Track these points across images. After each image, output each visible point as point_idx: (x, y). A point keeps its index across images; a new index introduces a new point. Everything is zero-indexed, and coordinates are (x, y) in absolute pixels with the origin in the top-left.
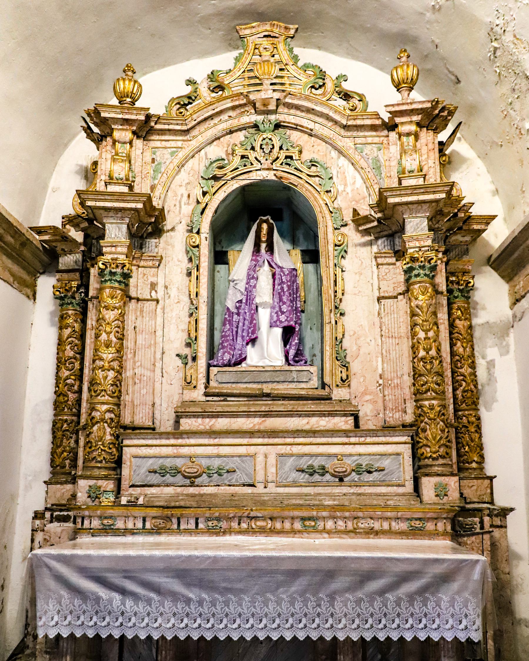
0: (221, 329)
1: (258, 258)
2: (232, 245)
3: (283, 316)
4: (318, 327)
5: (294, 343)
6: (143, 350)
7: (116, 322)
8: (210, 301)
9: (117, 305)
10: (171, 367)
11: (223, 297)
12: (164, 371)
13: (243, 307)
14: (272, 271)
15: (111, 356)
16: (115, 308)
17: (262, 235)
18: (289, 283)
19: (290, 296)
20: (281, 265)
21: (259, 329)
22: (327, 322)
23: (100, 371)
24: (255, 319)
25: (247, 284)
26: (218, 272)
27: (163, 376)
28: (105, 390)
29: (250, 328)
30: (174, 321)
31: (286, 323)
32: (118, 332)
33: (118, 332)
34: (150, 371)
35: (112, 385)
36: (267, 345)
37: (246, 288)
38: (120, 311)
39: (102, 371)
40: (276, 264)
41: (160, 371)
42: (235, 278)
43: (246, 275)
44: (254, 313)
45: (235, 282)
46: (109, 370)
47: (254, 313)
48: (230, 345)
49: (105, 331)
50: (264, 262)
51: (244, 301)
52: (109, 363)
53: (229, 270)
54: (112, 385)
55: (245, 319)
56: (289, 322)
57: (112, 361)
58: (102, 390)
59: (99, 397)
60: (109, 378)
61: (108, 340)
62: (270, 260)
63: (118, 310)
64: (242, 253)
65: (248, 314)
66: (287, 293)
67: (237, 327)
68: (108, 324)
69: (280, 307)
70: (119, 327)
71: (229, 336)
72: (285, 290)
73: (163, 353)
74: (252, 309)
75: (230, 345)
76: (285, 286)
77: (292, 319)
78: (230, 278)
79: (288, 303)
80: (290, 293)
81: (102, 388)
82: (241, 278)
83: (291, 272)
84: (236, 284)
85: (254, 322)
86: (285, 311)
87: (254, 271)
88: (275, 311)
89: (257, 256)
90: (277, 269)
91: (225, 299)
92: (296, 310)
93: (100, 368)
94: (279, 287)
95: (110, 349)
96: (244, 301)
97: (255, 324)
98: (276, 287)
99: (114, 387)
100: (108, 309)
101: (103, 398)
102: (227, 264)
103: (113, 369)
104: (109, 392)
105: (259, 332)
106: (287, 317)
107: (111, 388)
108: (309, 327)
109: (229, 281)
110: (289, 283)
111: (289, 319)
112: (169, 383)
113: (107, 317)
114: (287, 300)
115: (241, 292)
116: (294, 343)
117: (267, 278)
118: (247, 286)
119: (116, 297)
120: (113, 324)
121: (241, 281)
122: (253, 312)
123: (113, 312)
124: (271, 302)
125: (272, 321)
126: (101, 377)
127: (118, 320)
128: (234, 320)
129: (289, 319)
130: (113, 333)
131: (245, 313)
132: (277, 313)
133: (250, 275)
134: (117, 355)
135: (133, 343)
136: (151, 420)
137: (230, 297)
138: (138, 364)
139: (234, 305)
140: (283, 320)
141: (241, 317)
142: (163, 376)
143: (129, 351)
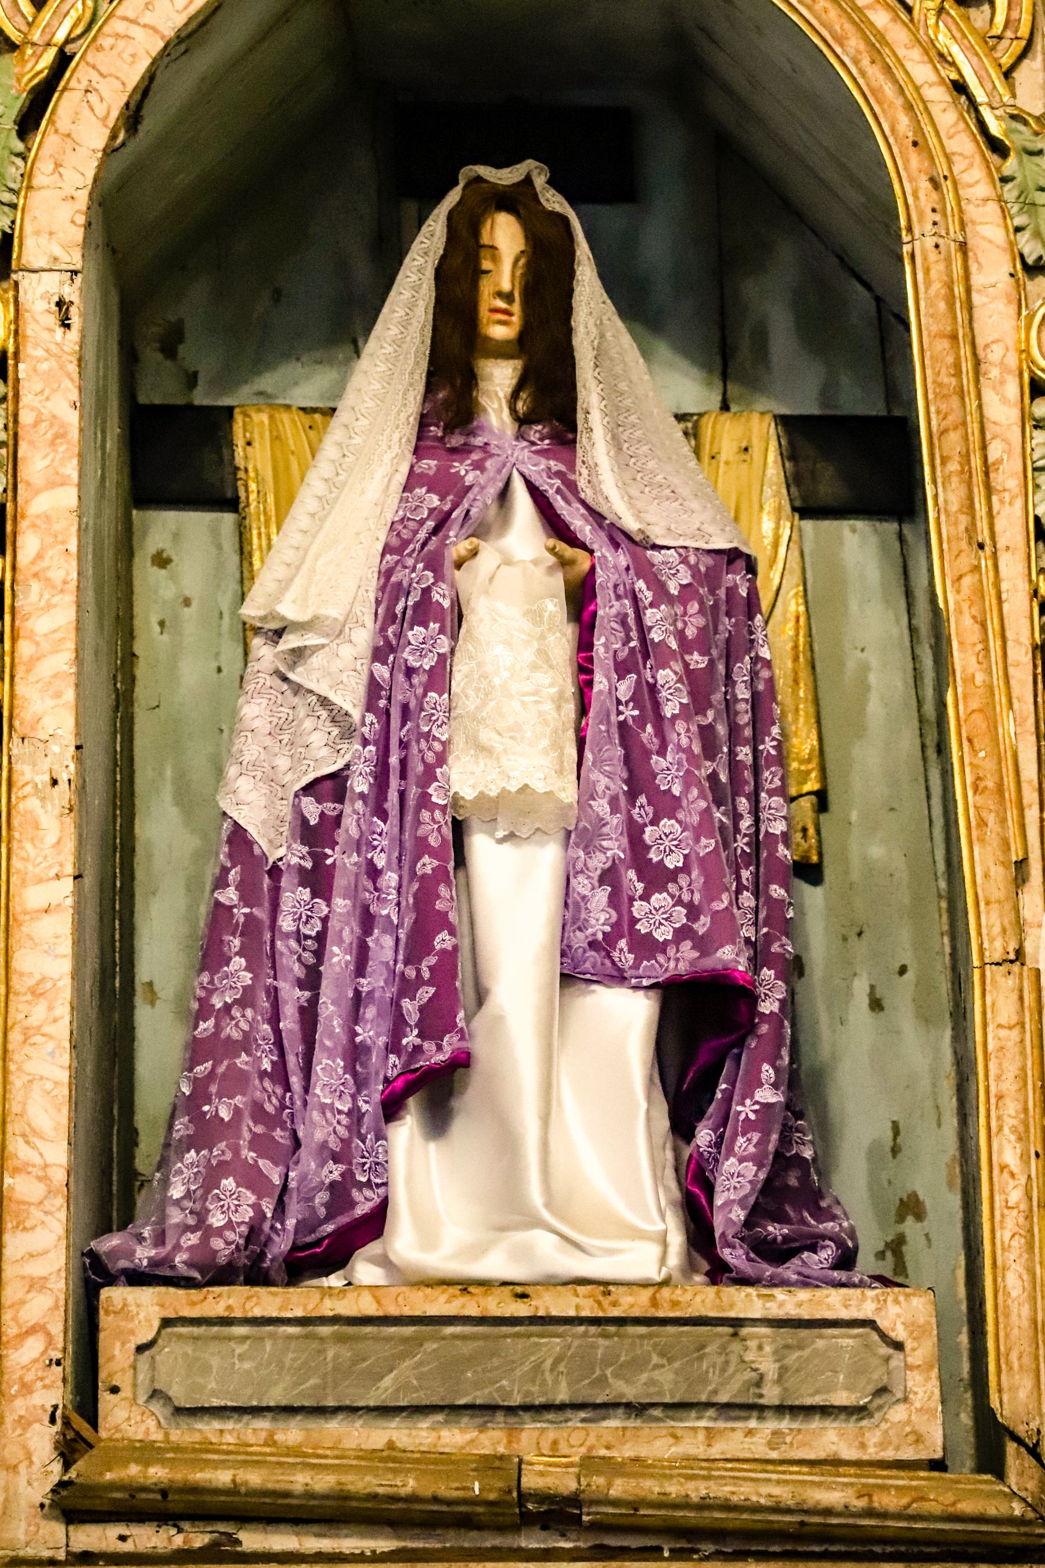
0: (180, 999)
1: (460, 468)
2: (260, 364)
3: (659, 899)
4: (923, 985)
5: (746, 1110)
8: (98, 782)
11: (198, 759)
13: (350, 826)
14: (564, 563)
17: (488, 301)
18: (697, 660)
19: (710, 750)
20: (631, 524)
21: (481, 997)
22: (996, 950)
24: (444, 923)
25: (379, 655)
26: (161, 561)
29: (407, 988)
31: (687, 950)
36: (546, 1119)
37: (374, 687)
40: (596, 516)
42: (289, 610)
43: (372, 584)
44: (440, 875)
45: (290, 641)
47: (440, 875)
48: (258, 1112)
50: (504, 495)
51: (360, 784)
53: (244, 552)
55: (367, 920)
56: (704, 945)
62: (550, 487)
64: (336, 432)
65: (390, 879)
66: (683, 734)
67: (312, 980)
69: (634, 833)
71: (246, 1044)
72: (670, 710)
74: (422, 846)
75: (258, 1112)
76: (666, 676)
77: (726, 924)
78: (251, 610)
79: (696, 803)
80: (706, 733)
82: (334, 612)
83: (711, 579)
84: (298, 655)
85: (442, 941)
86: (673, 862)
87: (434, 564)
88: (598, 862)
89: (462, 451)
90: (603, 550)
91: (219, 773)
92: (754, 857)
94: (625, 688)
96: (360, 784)
97: (450, 957)
98: (601, 682)
102: (232, 504)
105: (477, 1023)
106: (693, 912)
108: (861, 988)
109: (247, 631)
110: (697, 660)
111: (702, 925)
114: (688, 780)
115: (338, 717)
116: (746, 1110)
117: (535, 616)
118: (382, 672)
121: (339, 632)
122: (427, 865)
124: (569, 794)
125: (579, 940)
128: (286, 924)
129: (702, 925)
131: (374, 873)
132: (609, 877)
133: (400, 591)
137: (250, 749)
139: (285, 810)
140: (664, 934)
141: (341, 904)
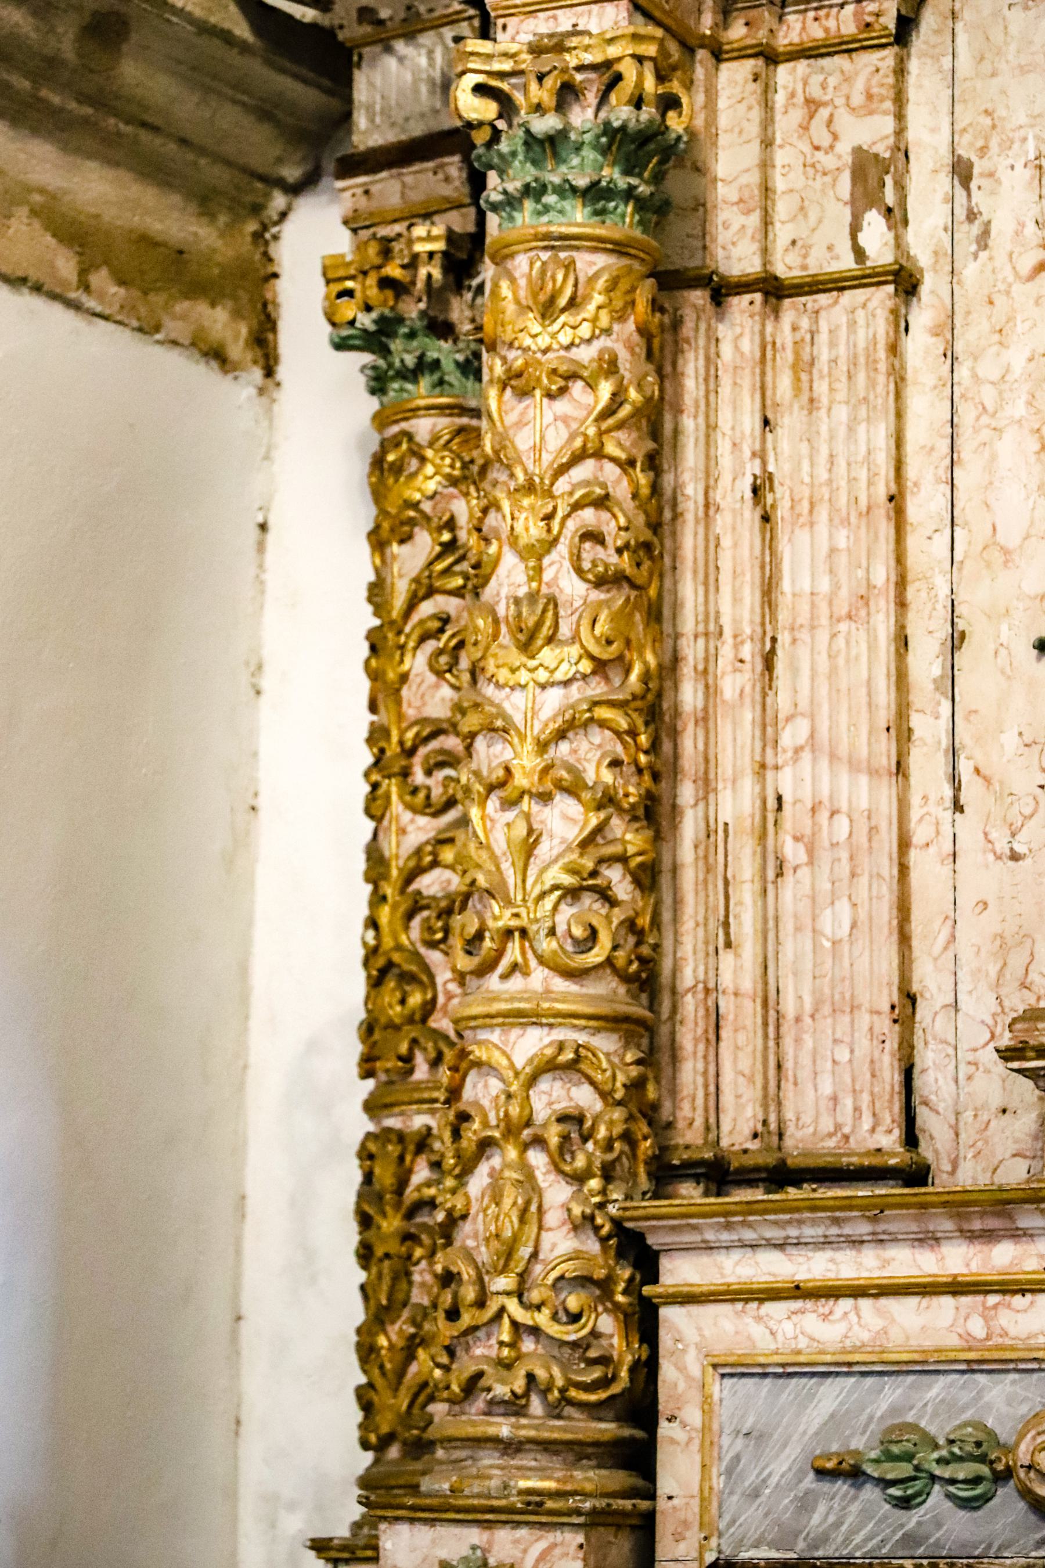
6: (823, 636)
7: (584, 470)
9: (585, 354)
10: (1010, 740)
12: (965, 768)
15: (553, 701)
16: (573, 376)
23: (493, 804)
27: (958, 807)
28: (524, 932)
30: (1019, 409)
32: (593, 536)
33: (593, 536)
34: (873, 772)
35: (573, 893)
38: (606, 389)
39: (509, 804)
41: (941, 765)
46: (545, 798)
49: (513, 539)
52: (542, 747)
54: (573, 893)
57: (561, 735)
58: (508, 933)
59: (493, 982)
60: (545, 850)
61: (533, 597)
63: (591, 386)
68: (530, 488)
70: (602, 502)
73: (956, 641)
81: (506, 920)
93: (491, 788)
95: (547, 655)
99: (588, 900)
100: (524, 393)
101: (517, 983)
103: (574, 787)
104: (547, 945)
107: (567, 911)
112: (1002, 846)
113: (523, 441)
119: (573, 303)
120: (562, 485)
123: (561, 406)
126: (499, 842)
127: (599, 454)
130: (562, 549)
134: (597, 688)
135: (751, 597)
136: (892, 1113)
138: (792, 735)
142: (958, 807)
143: (727, 651)
